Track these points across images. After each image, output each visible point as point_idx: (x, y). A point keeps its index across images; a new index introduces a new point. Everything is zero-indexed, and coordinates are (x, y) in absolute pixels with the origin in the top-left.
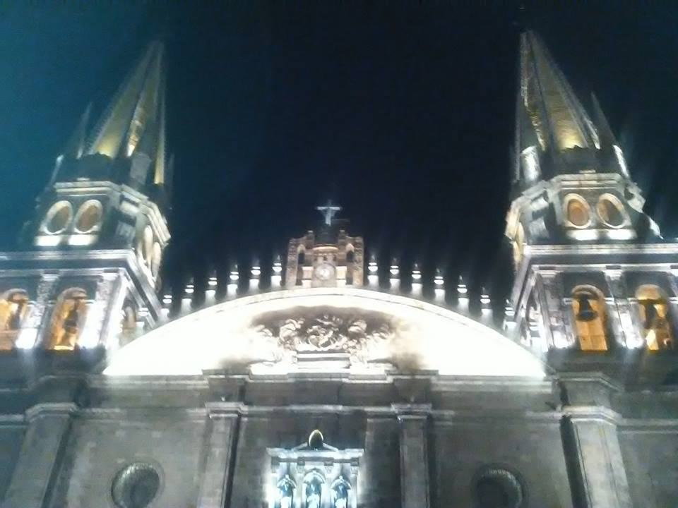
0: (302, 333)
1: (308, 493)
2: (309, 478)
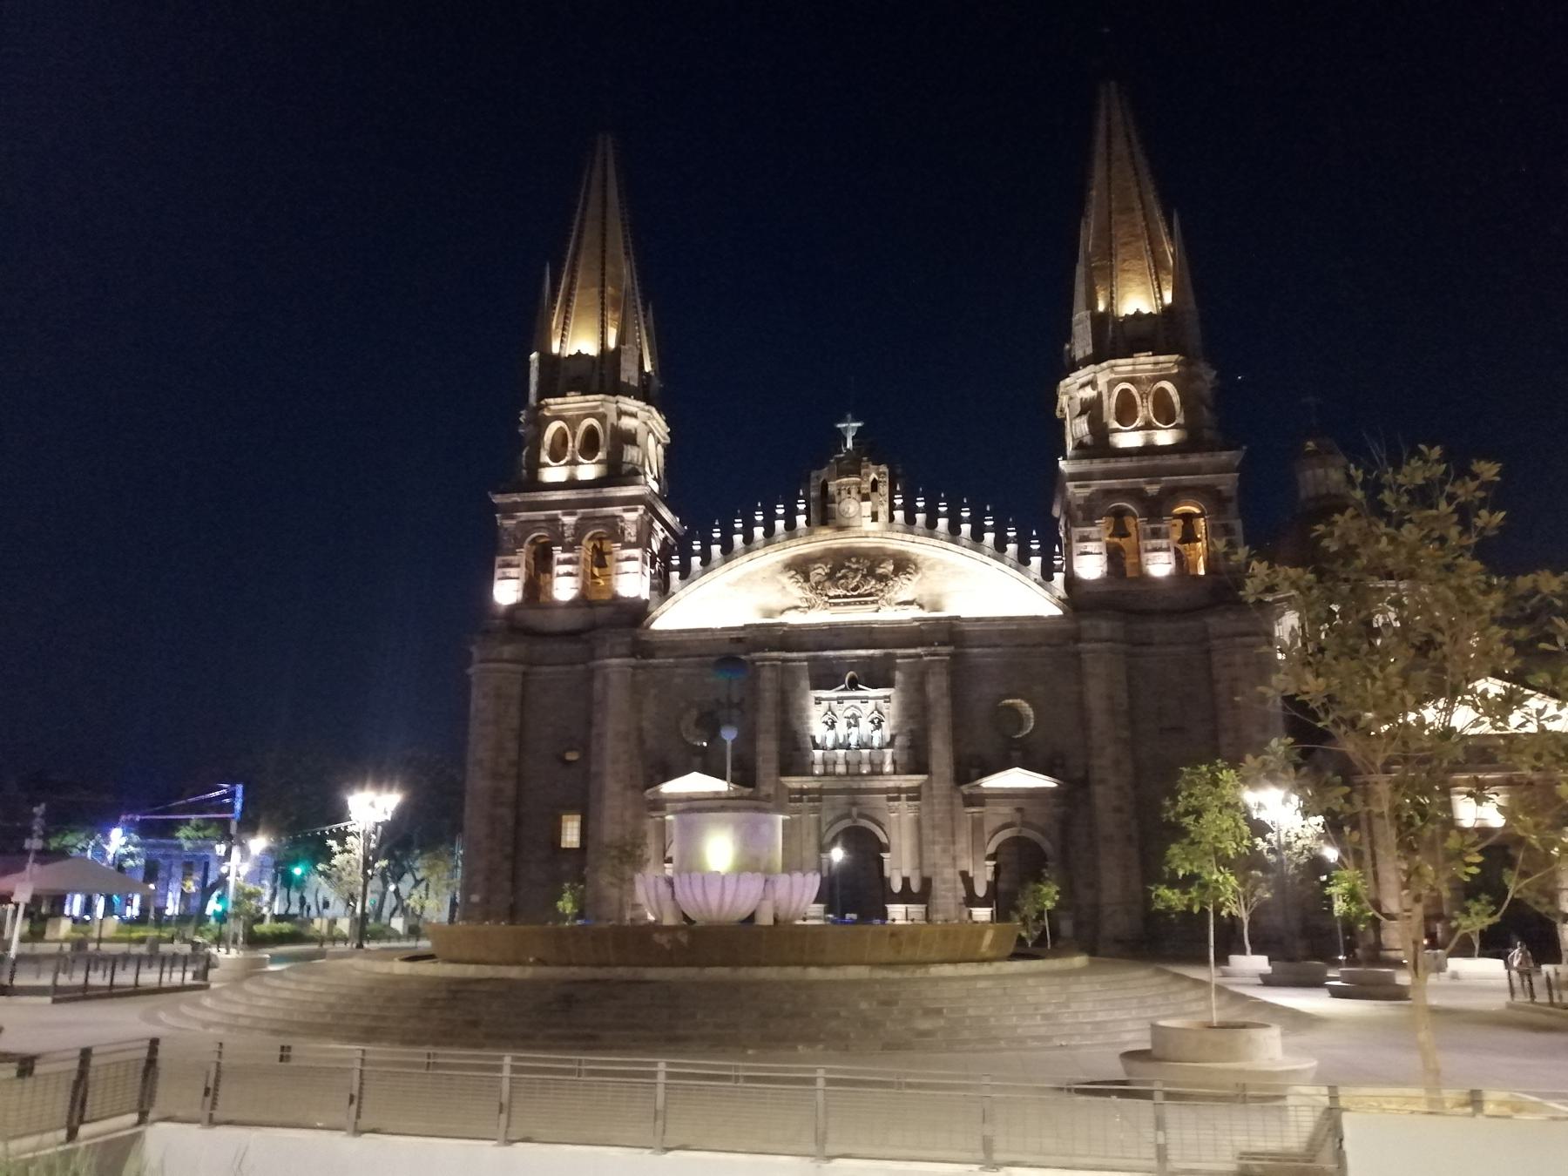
0: (831, 576)
1: (849, 726)
2: (849, 713)
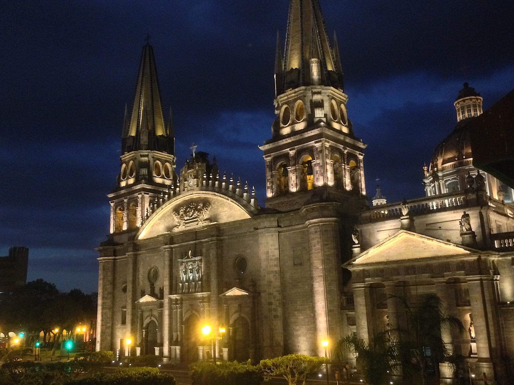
0: (185, 212)
